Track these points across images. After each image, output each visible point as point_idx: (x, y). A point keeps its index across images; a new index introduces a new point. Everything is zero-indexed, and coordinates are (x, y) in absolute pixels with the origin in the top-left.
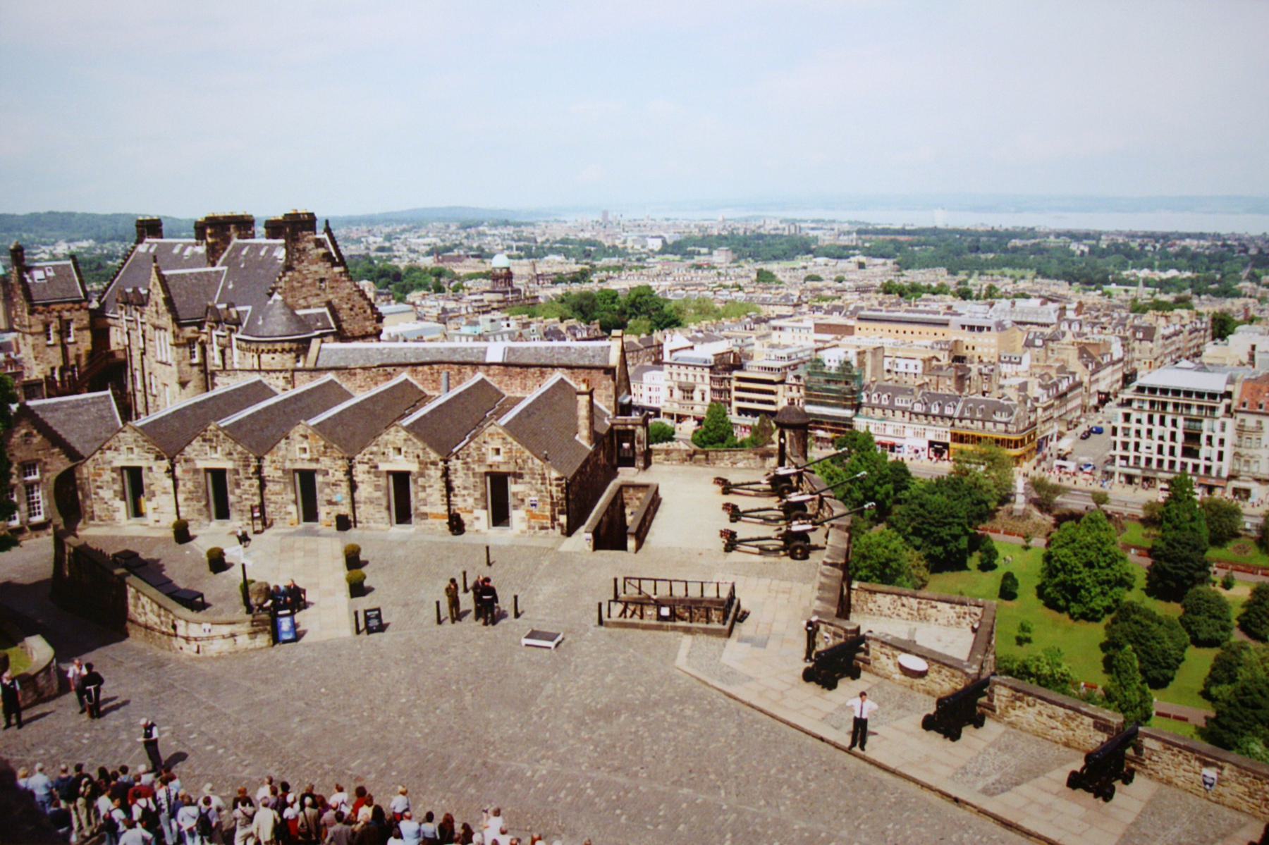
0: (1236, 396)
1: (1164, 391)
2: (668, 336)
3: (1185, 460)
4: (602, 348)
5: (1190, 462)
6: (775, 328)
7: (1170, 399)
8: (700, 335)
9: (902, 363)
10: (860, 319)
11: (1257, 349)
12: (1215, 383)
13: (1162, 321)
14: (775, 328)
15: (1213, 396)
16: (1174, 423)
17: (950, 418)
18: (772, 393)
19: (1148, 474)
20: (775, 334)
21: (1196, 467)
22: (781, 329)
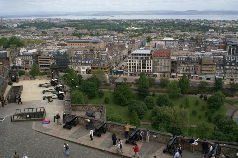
0: (152, 55)
1: (138, 54)
2: (21, 49)
3: (143, 69)
4: (5, 53)
5: (144, 70)
6: (48, 45)
7: (139, 57)
8: (29, 48)
9: (78, 52)
10: (68, 42)
11: (157, 44)
12: (148, 52)
13: (136, 39)
14: (48, 45)
15: (148, 55)
16: (140, 62)
17: (91, 64)
18: (48, 61)
19: (135, 73)
20: (48, 47)
21: (145, 70)
22: (49, 45)
